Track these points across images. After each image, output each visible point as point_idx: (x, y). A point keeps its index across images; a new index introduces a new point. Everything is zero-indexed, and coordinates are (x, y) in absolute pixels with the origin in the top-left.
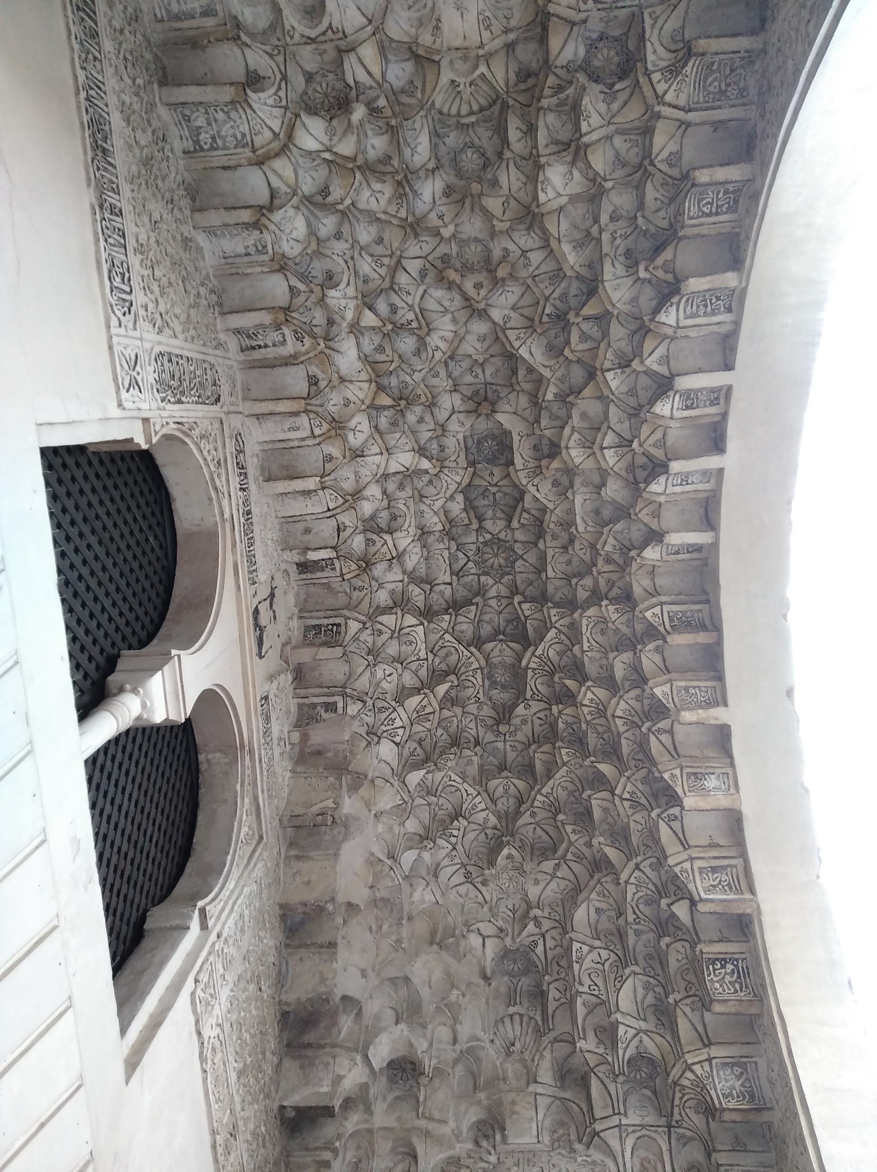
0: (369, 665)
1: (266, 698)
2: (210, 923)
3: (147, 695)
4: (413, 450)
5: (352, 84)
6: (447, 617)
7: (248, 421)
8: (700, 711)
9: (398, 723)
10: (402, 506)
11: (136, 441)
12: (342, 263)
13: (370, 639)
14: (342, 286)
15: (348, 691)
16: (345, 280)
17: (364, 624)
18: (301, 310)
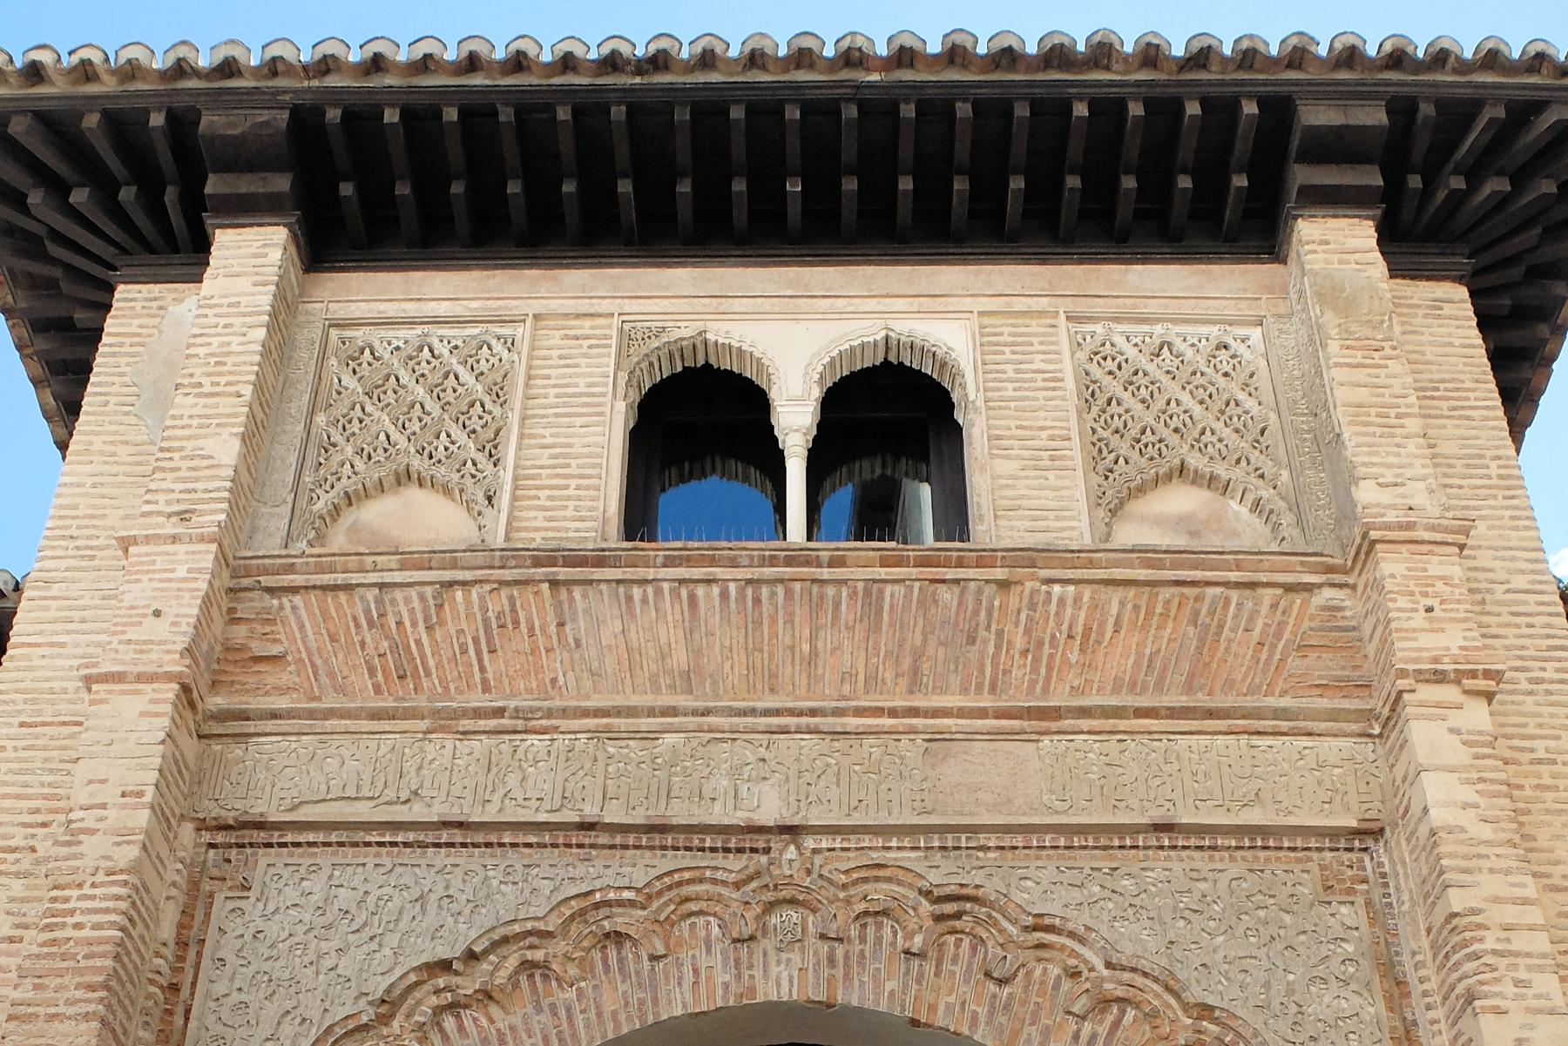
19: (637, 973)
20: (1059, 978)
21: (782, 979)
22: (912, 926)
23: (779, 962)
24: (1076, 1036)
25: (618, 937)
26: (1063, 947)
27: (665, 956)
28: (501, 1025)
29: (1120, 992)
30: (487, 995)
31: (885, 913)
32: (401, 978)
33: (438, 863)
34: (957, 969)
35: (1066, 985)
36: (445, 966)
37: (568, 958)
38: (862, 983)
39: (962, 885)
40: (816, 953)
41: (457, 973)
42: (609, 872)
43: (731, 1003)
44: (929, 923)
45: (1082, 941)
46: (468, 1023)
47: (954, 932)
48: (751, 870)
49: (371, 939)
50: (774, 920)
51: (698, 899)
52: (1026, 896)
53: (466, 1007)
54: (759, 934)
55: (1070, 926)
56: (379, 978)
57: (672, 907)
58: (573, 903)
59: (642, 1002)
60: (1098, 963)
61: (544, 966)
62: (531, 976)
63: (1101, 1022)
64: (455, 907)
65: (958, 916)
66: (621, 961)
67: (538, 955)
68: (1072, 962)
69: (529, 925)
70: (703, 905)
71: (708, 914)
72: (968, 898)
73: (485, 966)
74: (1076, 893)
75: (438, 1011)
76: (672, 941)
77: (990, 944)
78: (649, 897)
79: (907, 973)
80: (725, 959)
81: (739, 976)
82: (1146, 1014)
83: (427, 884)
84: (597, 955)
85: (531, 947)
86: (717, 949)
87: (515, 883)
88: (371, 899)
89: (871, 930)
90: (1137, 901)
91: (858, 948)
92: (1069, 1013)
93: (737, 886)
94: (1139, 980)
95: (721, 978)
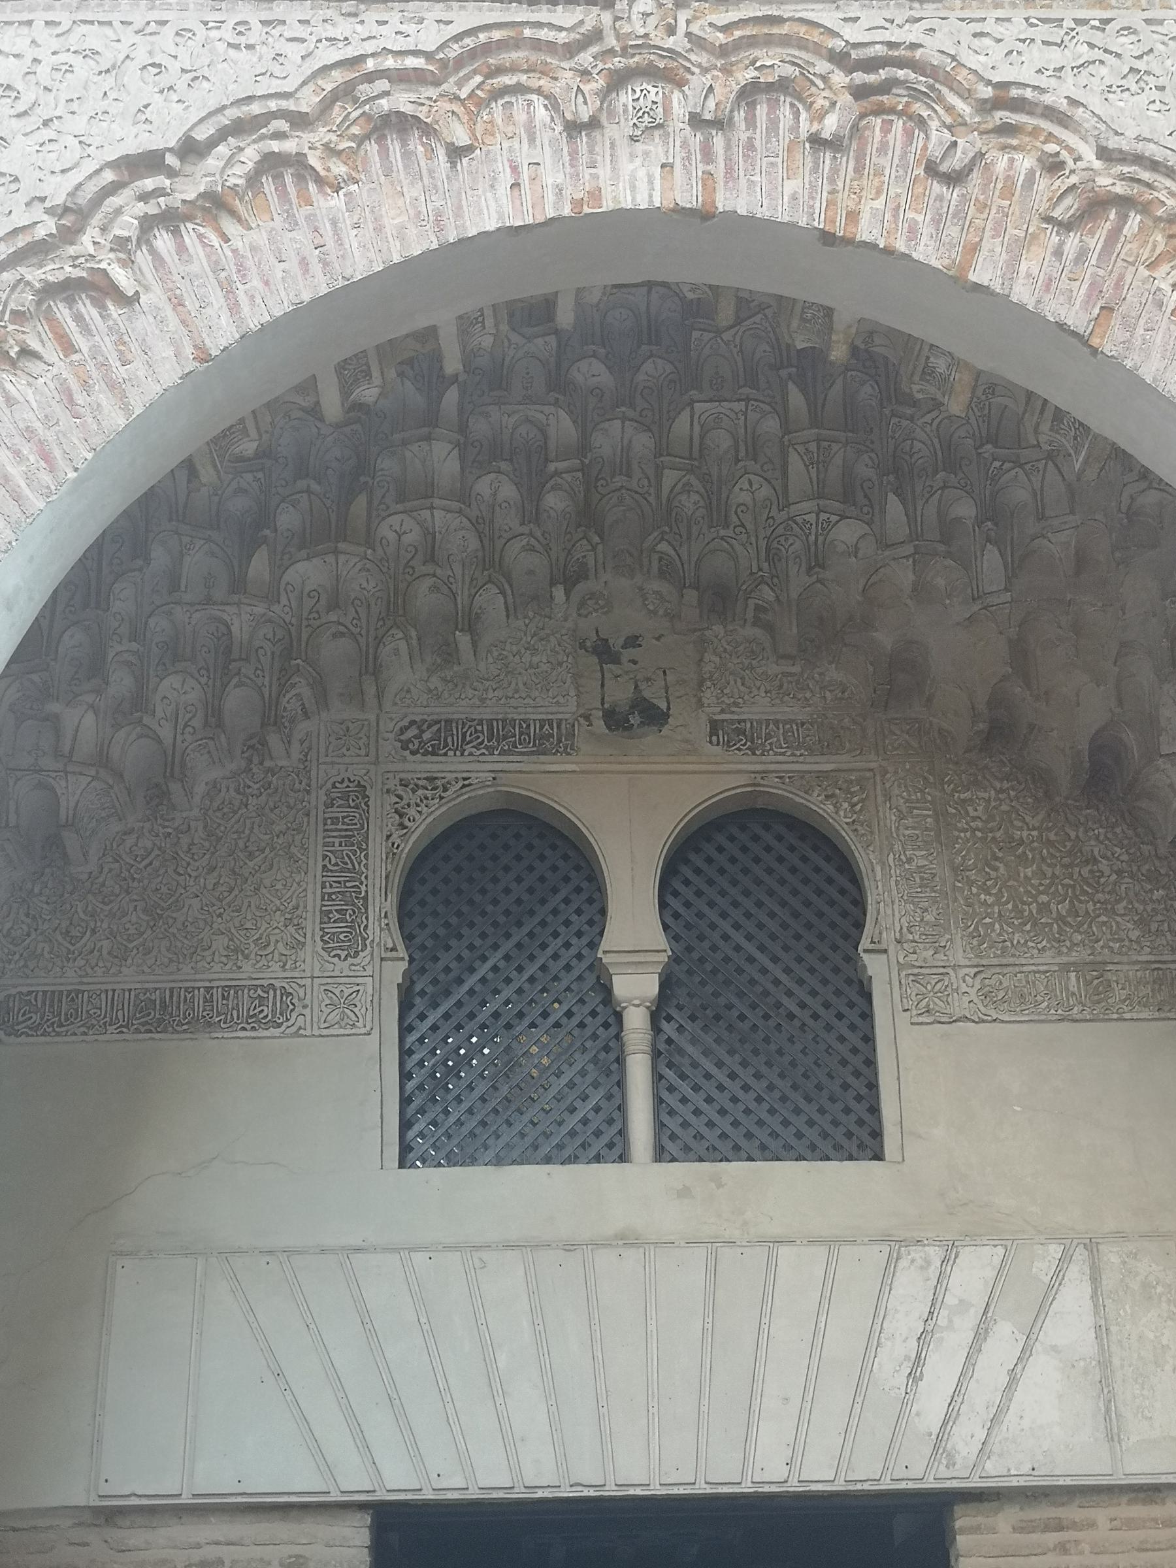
0: (722, 538)
1: (715, 727)
2: (884, 946)
3: (629, 1001)
4: (428, 438)
5: (20, 694)
6: (696, 334)
7: (387, 705)
8: (834, 338)
9: (811, 518)
10: (513, 420)
11: (400, 981)
12: (197, 615)
13: (696, 497)
14: (228, 619)
15: (744, 587)
16: (218, 613)
17: (662, 539)
18: (259, 681)
19: (431, 172)
20: (1031, 174)
21: (636, 178)
22: (820, 102)
23: (632, 156)
24: (1058, 253)
25: (401, 123)
26: (1035, 132)
27: (469, 149)
28: (237, 243)
29: (1120, 189)
30: (215, 205)
31: (783, 85)
32: (90, 177)
33: (138, 20)
34: (885, 162)
35: (1043, 183)
36: (151, 162)
37: (330, 150)
38: (751, 184)
39: (891, 45)
40: (685, 144)
41: (172, 173)
42: (383, 29)
43: (567, 211)
44: (846, 98)
45: (1063, 120)
46: (189, 239)
47: (880, 111)
48: (588, 26)
49: (46, 123)
50: (625, 98)
51: (513, 69)
52: (982, 58)
53: (189, 218)
54: (604, 120)
55: (1048, 99)
56: (59, 178)
57: (478, 79)
58: (335, 73)
59: (439, 214)
60: (1088, 153)
61: (298, 162)
62: (278, 177)
63: (1092, 233)
64: (165, 80)
65: (886, 87)
66: (407, 155)
67: (289, 146)
68: (1052, 148)
69: (273, 105)
70: (523, 78)
71: (530, 90)
72: (901, 63)
73: (213, 162)
74: (1055, 57)
75: (147, 224)
76: (479, 128)
77: (934, 124)
78: (444, 64)
79: (815, 169)
80: (558, 152)
81: (576, 177)
82: (1160, 219)
83: (123, 49)
84: (372, 148)
85: (279, 136)
86: (544, 137)
87: (249, 47)
88: (43, 71)
89: (761, 111)
90: (1140, 65)
91: (744, 137)
92: (1048, 219)
93: (571, 50)
94: (1146, 176)
95: (552, 177)
